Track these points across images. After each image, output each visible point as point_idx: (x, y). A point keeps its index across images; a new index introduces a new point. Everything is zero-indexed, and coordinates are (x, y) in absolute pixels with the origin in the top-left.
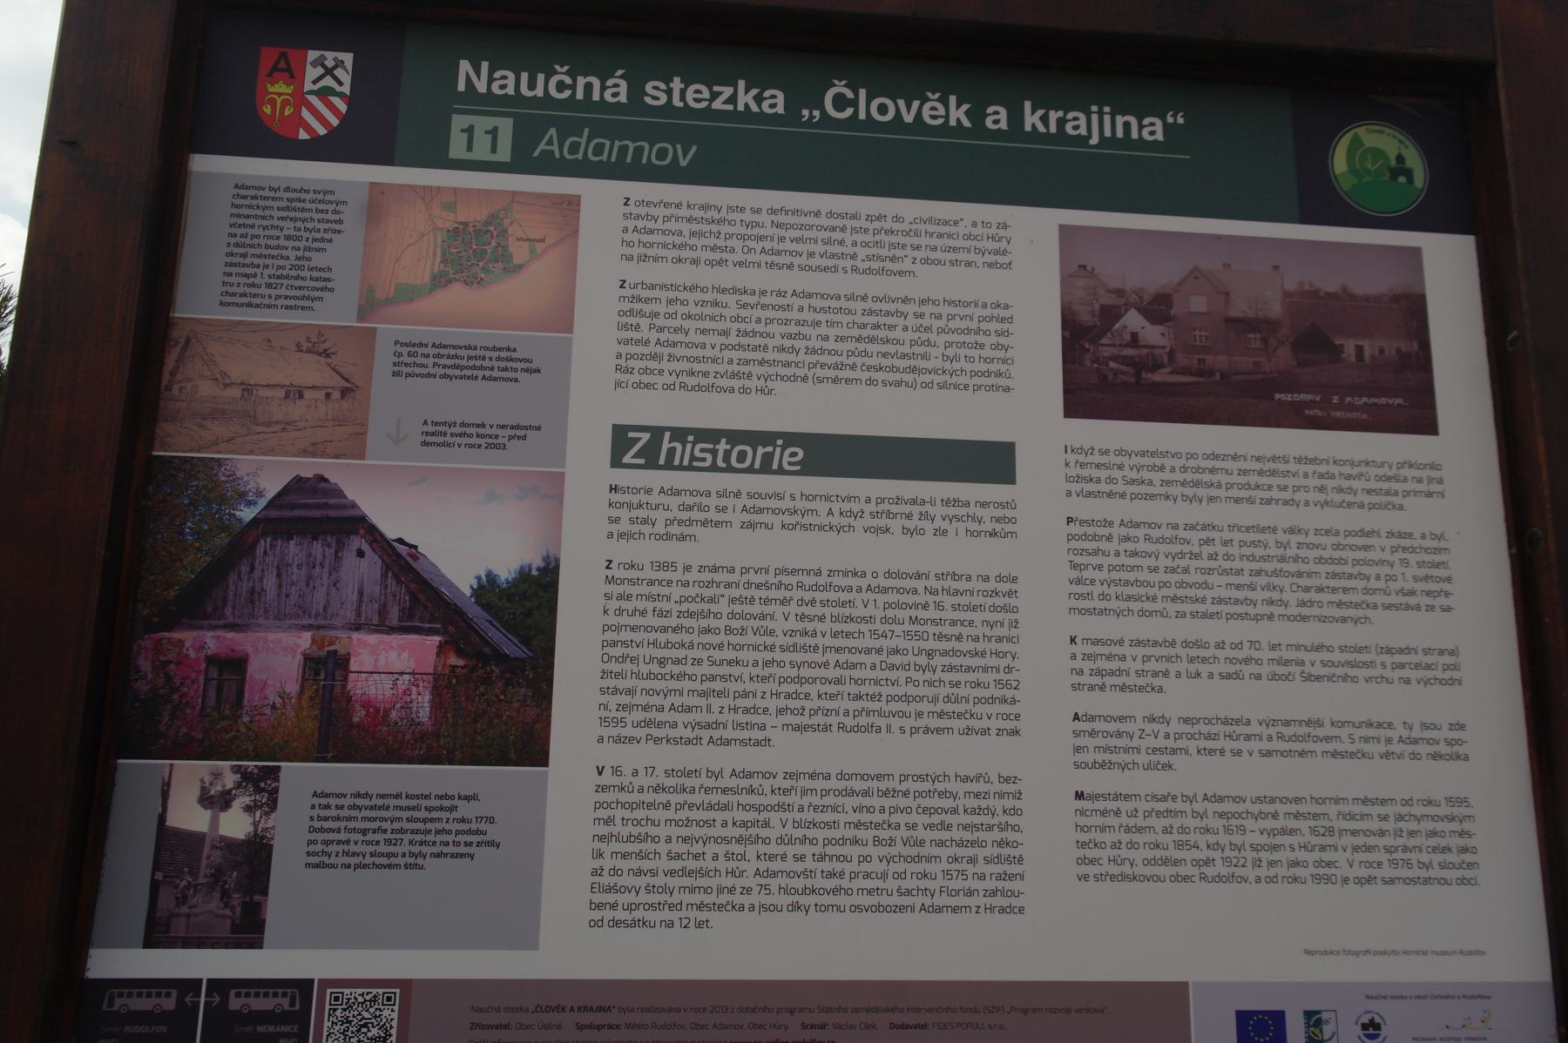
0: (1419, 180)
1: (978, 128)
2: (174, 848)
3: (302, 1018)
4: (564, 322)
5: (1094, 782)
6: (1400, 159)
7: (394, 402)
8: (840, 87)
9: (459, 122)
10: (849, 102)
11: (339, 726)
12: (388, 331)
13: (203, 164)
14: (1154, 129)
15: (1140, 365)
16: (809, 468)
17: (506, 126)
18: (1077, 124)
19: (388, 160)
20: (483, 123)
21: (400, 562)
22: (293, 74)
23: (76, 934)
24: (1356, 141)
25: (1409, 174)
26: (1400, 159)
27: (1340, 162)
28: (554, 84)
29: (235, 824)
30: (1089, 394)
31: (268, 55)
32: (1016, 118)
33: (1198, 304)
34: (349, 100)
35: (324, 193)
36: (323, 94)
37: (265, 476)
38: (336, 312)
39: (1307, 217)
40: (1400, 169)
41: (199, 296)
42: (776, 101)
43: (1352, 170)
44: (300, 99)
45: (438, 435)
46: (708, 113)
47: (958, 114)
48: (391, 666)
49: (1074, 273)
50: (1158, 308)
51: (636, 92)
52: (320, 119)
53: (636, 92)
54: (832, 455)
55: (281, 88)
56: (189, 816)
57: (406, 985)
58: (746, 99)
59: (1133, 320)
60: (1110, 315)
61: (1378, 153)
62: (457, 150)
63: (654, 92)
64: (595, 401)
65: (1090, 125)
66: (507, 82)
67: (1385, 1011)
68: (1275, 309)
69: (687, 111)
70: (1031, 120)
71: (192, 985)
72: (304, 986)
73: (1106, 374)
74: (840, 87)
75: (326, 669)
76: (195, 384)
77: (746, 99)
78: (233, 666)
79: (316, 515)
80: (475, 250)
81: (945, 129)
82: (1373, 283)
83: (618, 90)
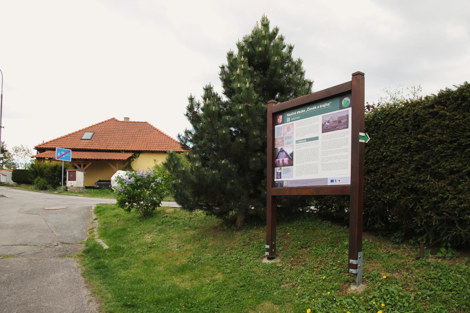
2: (277, 173)
4: (293, 133)
5: (323, 163)
7: (285, 141)
10: (310, 109)
11: (284, 165)
12: (285, 136)
13: (276, 126)
15: (327, 127)
16: (306, 141)
21: (286, 153)
23: (273, 178)
27: (343, 103)
28: (291, 114)
29: (280, 171)
30: (324, 131)
33: (331, 120)
35: (281, 127)
37: (279, 148)
38: (282, 136)
39: (340, 109)
41: (276, 137)
45: (288, 143)
48: (286, 160)
49: (323, 120)
50: (328, 122)
54: (308, 140)
56: (278, 171)
59: (327, 123)
60: (325, 123)
63: (297, 113)
64: (295, 139)
67: (340, 179)
68: (337, 119)
73: (325, 129)
75: (283, 160)
76: (276, 143)
78: (279, 161)
79: (282, 151)
80: (289, 129)
82: (344, 114)
83: (295, 113)
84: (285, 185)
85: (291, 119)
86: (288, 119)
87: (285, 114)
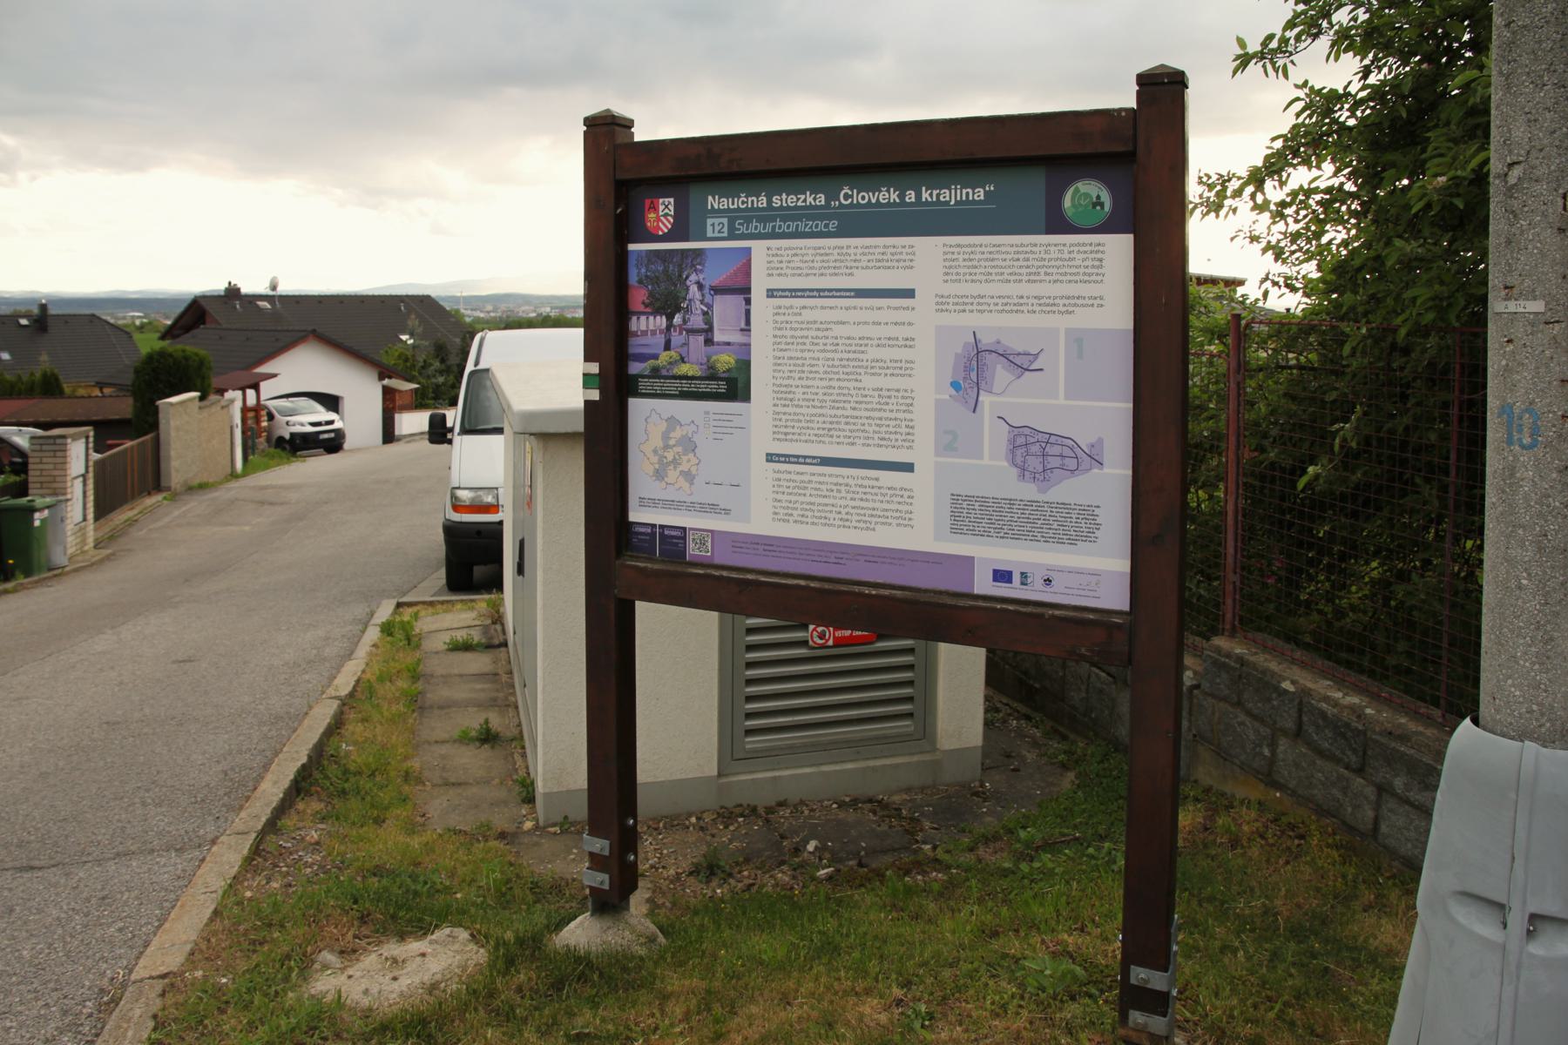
0: (1107, 208)
1: (903, 203)
3: (684, 538)
6: (1098, 197)
8: (846, 190)
9: (709, 221)
10: (852, 196)
13: (632, 247)
14: (980, 194)
17: (725, 221)
18: (945, 195)
19: (687, 240)
20: (717, 221)
22: (656, 209)
24: (1077, 190)
25: (1102, 205)
26: (1098, 197)
27: (1067, 202)
31: (648, 202)
32: (919, 196)
34: (675, 217)
36: (666, 216)
40: (1098, 203)
42: (821, 199)
43: (1073, 205)
44: (658, 219)
46: (796, 208)
47: (894, 197)
51: (770, 202)
52: (665, 226)
53: (770, 202)
55: (652, 215)
57: (712, 532)
58: (810, 200)
61: (1087, 195)
62: (710, 234)
65: (951, 195)
66: (725, 203)
69: (789, 208)
70: (925, 195)
71: (654, 526)
72: (684, 529)
74: (846, 190)
77: (810, 200)
81: (889, 204)
84: (693, 550)
85: (732, 228)
86: (714, 225)
87: (694, 192)
